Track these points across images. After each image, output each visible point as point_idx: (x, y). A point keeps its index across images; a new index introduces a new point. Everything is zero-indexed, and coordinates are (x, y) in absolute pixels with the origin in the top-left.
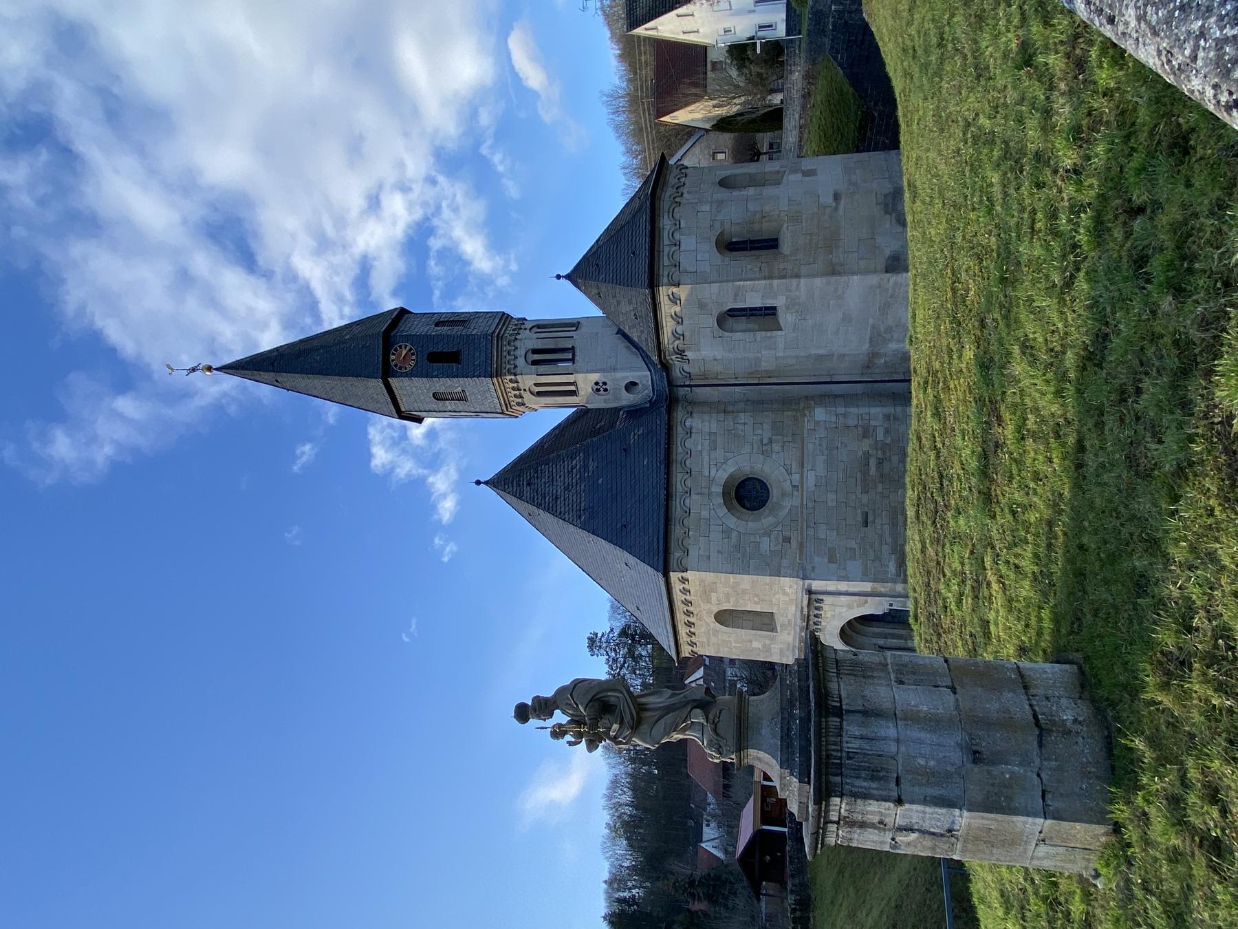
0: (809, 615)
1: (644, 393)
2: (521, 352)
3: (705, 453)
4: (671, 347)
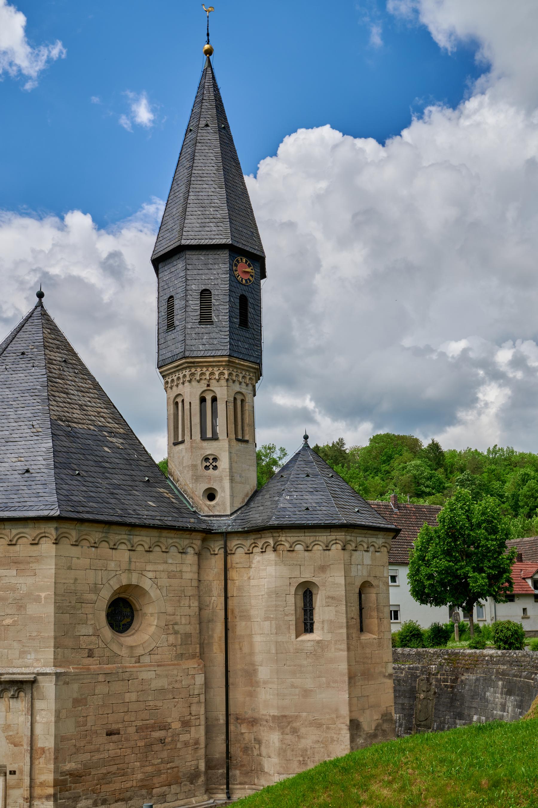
4: (283, 539)
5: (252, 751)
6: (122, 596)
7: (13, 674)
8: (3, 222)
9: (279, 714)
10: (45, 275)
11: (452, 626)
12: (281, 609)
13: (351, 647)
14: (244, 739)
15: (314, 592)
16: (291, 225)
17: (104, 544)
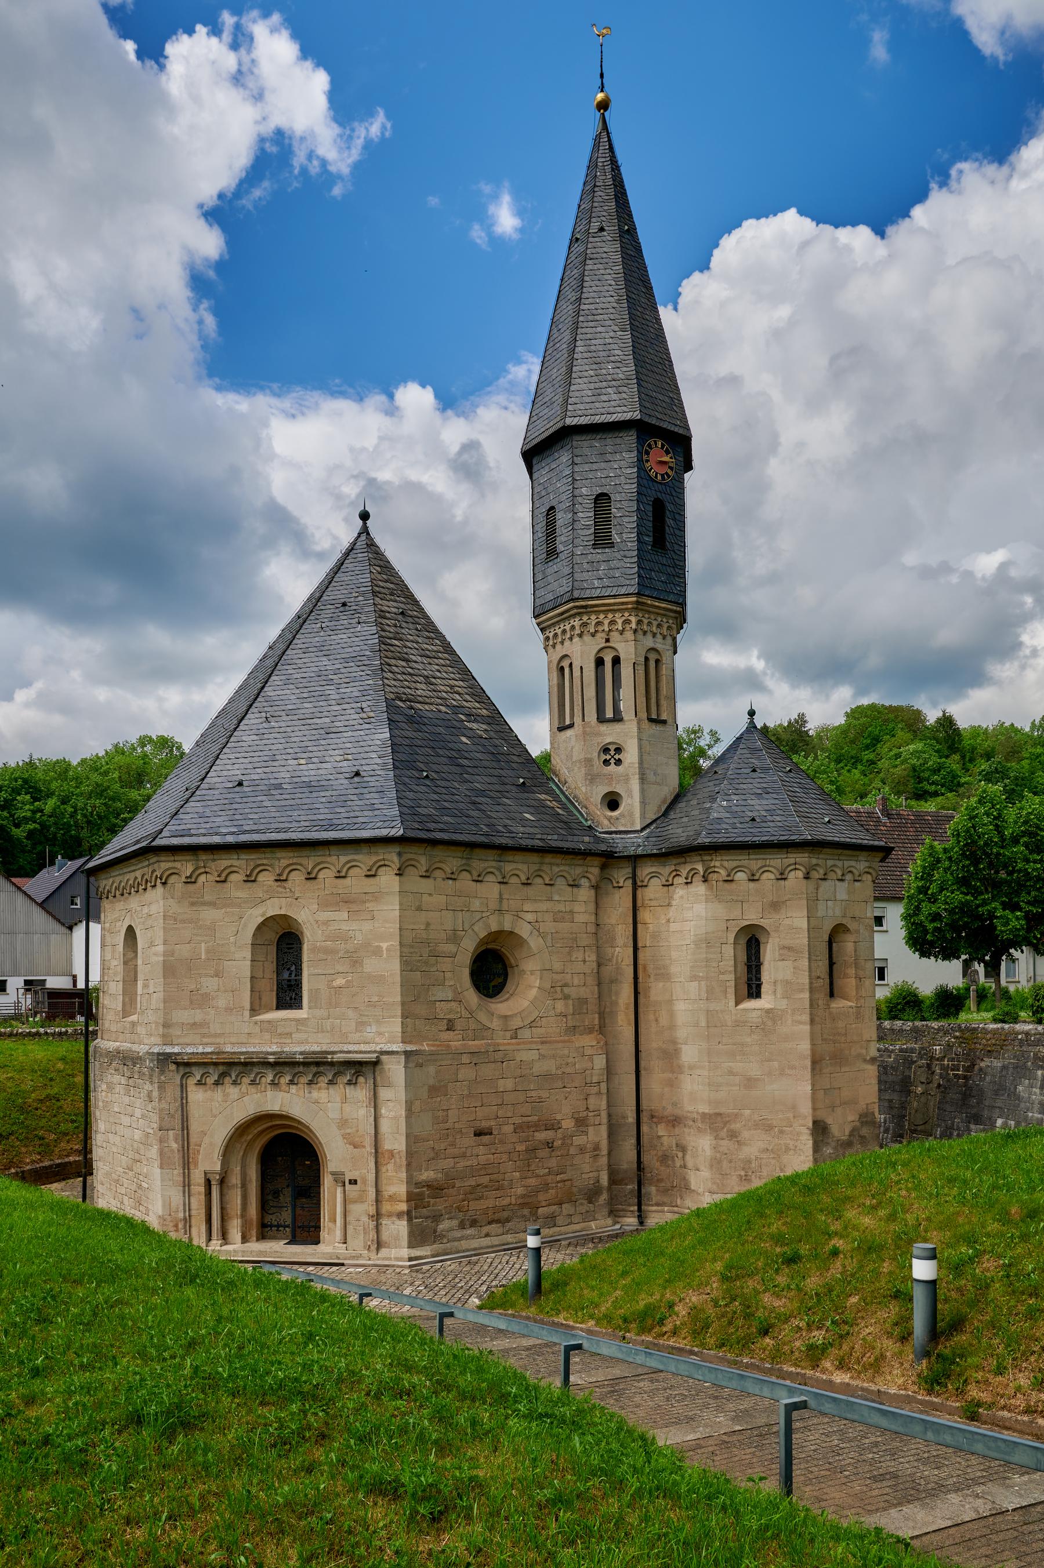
1: (604, 820)
4: (717, 864)
5: (673, 1161)
6: (490, 947)
7: (349, 1052)
8: (308, 407)
9: (711, 1112)
10: (372, 482)
11: (968, 989)
12: (715, 964)
13: (817, 1019)
14: (662, 1144)
15: (762, 940)
16: (733, 381)
17: (465, 874)
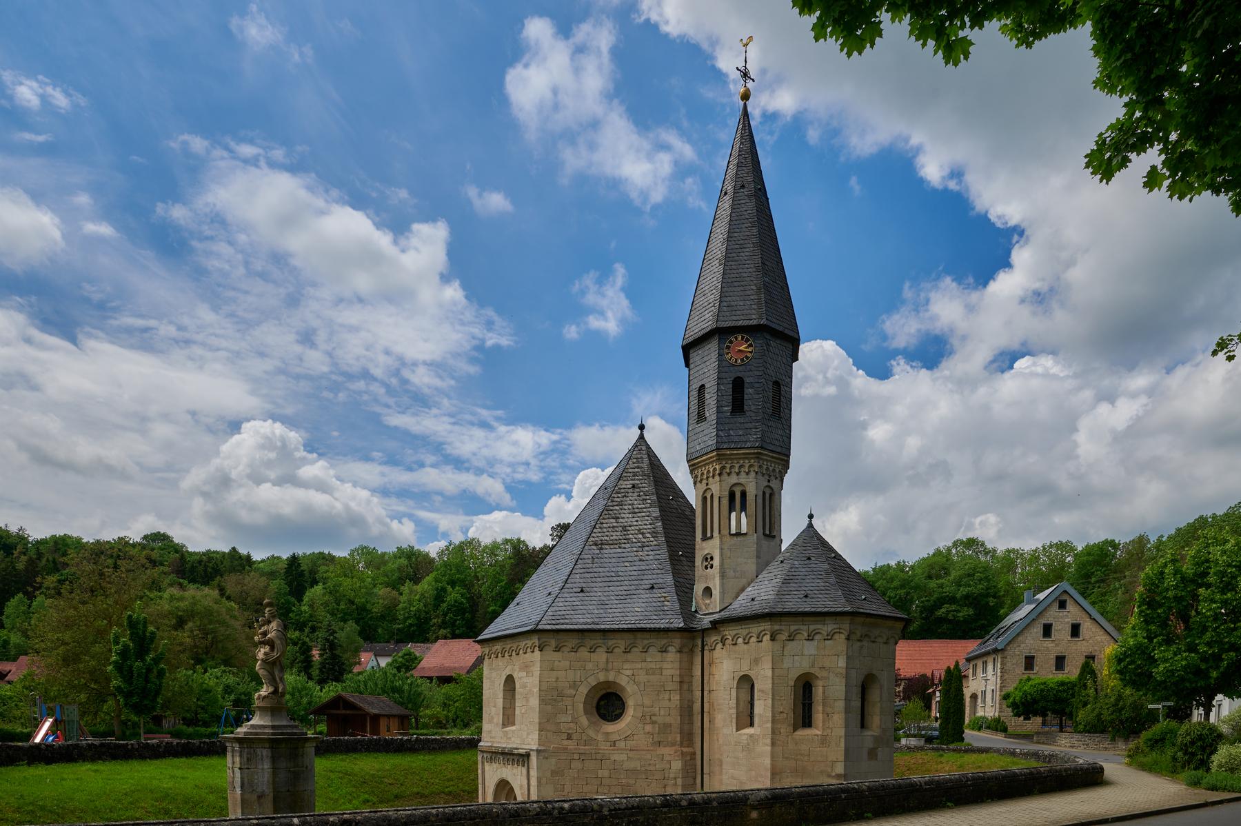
0: (513, 754)
2: (743, 479)
3: (644, 665)
6: (608, 691)
